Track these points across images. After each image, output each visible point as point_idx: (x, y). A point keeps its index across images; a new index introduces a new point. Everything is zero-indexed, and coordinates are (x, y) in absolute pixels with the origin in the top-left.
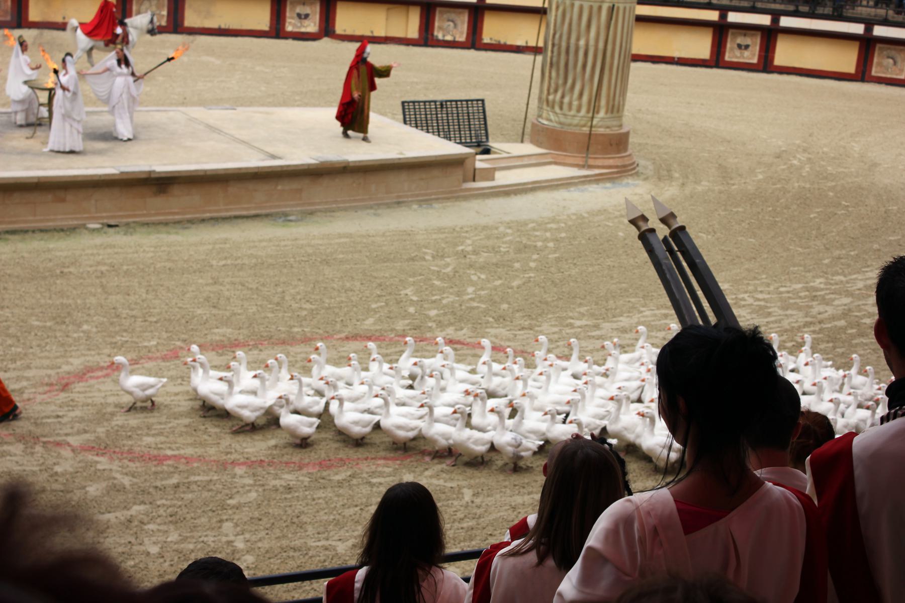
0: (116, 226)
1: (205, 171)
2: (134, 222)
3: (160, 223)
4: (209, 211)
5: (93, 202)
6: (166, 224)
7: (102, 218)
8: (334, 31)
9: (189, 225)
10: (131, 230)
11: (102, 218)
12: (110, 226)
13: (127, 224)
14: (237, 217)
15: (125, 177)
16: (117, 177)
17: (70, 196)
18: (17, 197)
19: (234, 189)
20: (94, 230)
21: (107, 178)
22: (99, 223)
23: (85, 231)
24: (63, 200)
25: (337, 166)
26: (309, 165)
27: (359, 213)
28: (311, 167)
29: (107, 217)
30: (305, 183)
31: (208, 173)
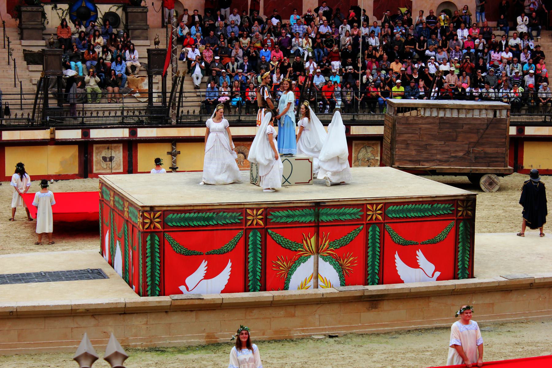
0: (337, 336)
1: (410, 289)
2: (351, 333)
3: (372, 334)
4: (414, 323)
5: (317, 316)
6: (378, 335)
7: (325, 330)
8: (522, 167)
9: (397, 335)
10: (349, 340)
11: (325, 330)
12: (331, 337)
13: (345, 335)
14: (437, 328)
15: (343, 295)
16: (336, 296)
17: (299, 312)
18: (256, 312)
19: (434, 304)
20: (318, 340)
21: (328, 296)
22: (322, 334)
23: (311, 341)
24: (294, 316)
25: (524, 283)
26: (499, 282)
27: (546, 323)
28: (501, 284)
29: (329, 329)
30: (496, 298)
31: (412, 291)
